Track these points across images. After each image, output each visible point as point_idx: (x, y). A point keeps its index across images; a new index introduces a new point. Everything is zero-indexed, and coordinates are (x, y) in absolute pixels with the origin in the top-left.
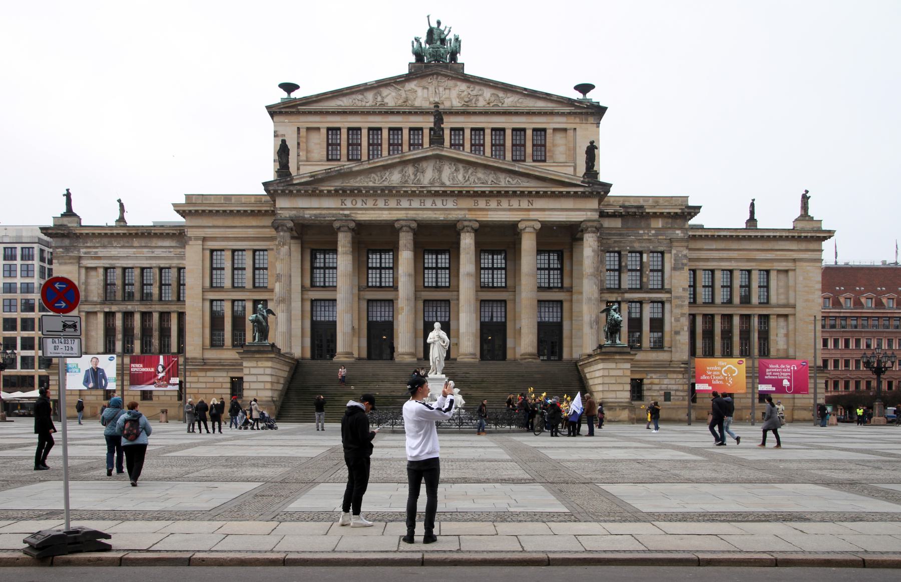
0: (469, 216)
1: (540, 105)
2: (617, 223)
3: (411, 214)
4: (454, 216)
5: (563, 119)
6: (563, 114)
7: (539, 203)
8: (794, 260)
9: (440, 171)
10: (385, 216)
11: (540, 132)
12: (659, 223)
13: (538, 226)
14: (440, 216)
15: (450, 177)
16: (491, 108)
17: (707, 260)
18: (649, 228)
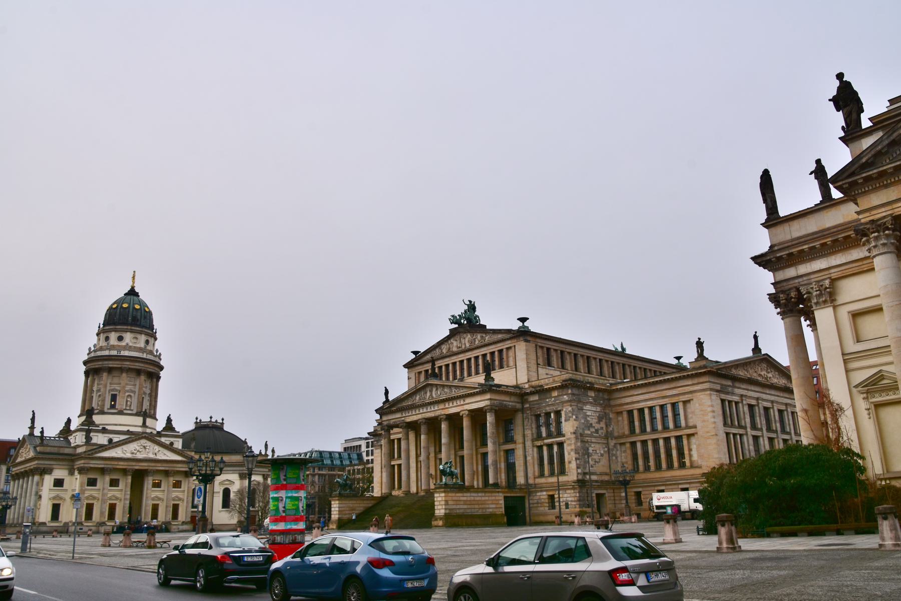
0: (443, 412)
1: (500, 336)
2: (536, 397)
3: (424, 416)
4: (438, 413)
5: (509, 342)
6: (508, 339)
7: (468, 400)
8: (691, 392)
9: (431, 391)
10: (415, 418)
11: (501, 351)
12: (555, 394)
13: (467, 412)
14: (432, 415)
15: (436, 394)
16: (480, 344)
17: (638, 402)
18: (551, 397)
